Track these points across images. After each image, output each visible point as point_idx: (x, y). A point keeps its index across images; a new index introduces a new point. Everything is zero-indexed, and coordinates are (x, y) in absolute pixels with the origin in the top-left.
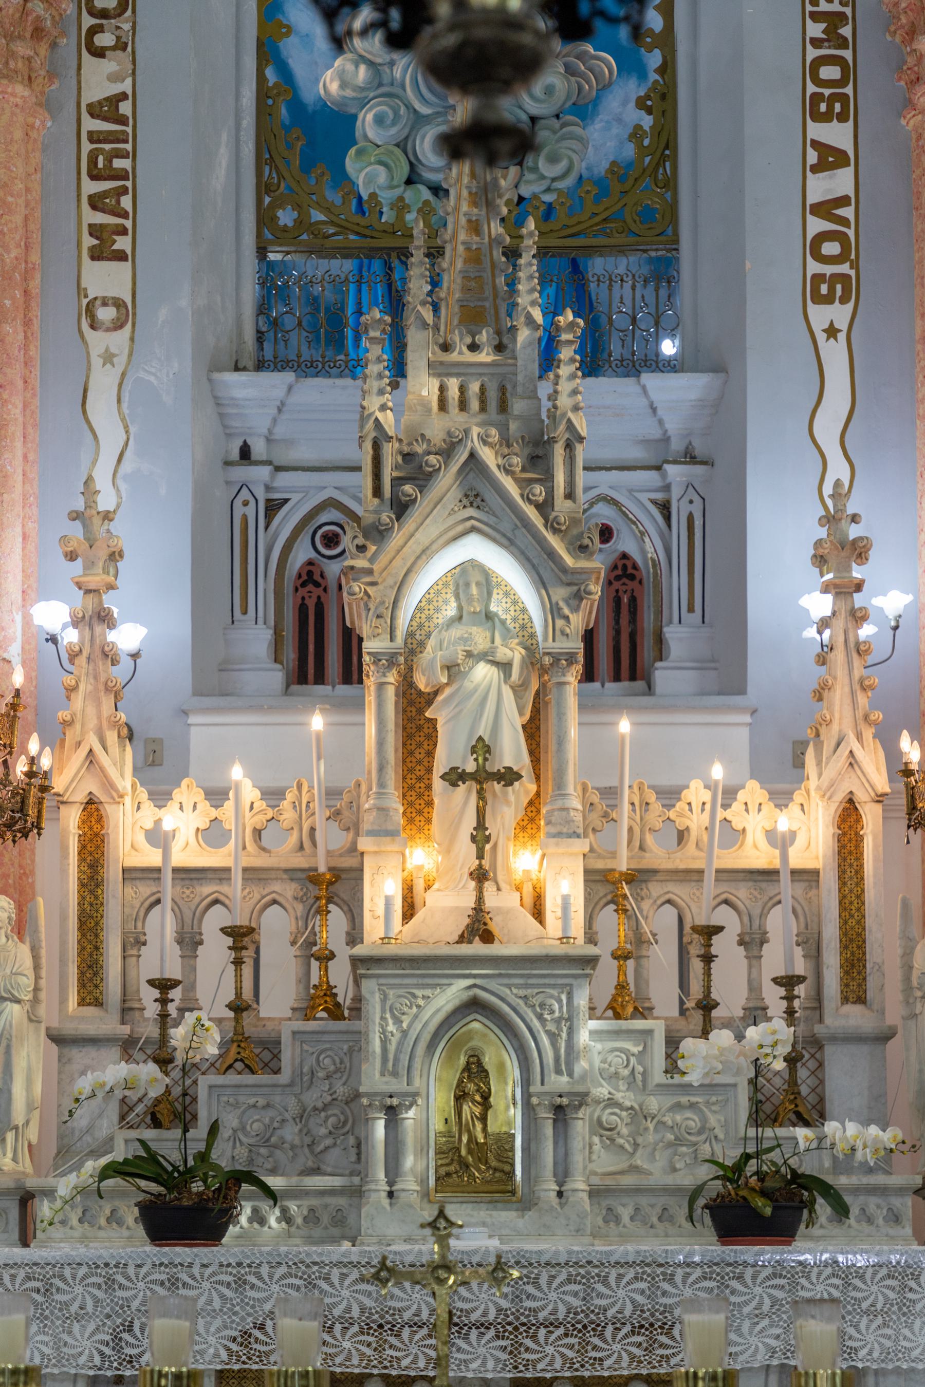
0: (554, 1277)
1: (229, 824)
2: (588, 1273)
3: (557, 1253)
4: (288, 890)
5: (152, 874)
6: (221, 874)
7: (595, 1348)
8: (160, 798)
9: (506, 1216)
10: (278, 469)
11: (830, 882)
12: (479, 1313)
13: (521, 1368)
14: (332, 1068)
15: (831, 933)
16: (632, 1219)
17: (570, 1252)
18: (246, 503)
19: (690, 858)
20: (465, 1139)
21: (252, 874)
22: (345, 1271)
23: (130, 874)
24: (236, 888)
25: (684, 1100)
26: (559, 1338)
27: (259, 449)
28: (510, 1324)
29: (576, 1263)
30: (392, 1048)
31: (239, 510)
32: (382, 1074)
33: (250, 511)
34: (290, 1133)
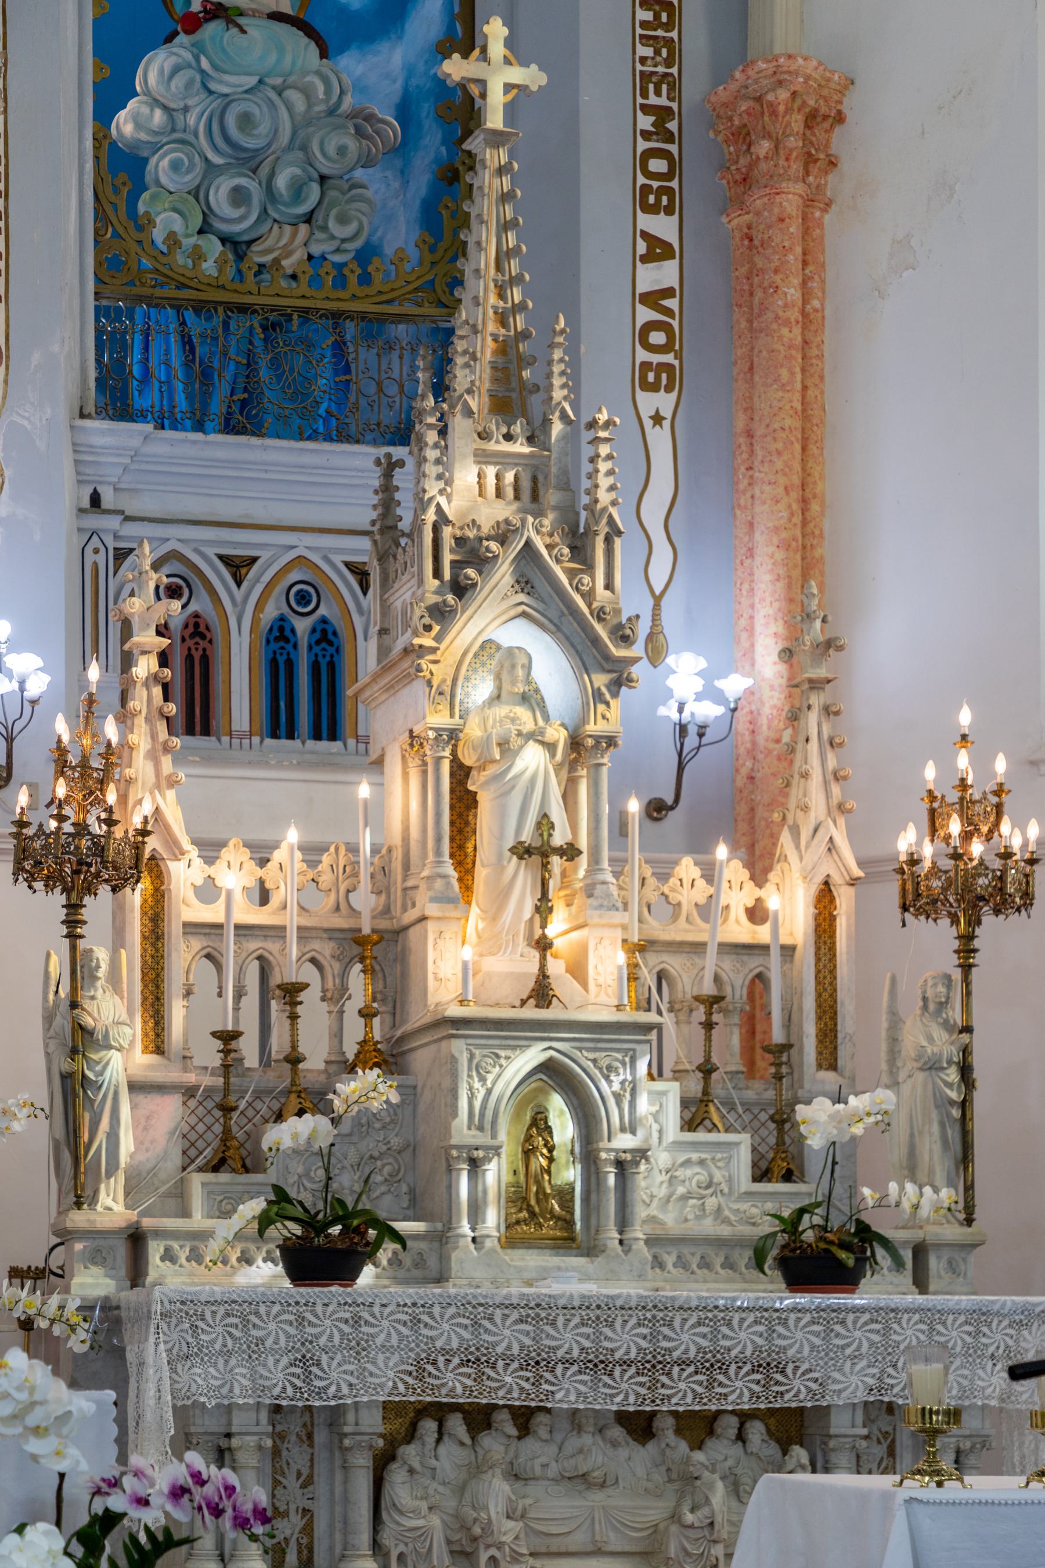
0: (686, 1320)
2: (715, 1316)
3: (689, 1298)
7: (720, 1384)
10: (128, 519)
12: (621, 1352)
13: (658, 1402)
14: (388, 1120)
16: (675, 1266)
17: (699, 1298)
18: (96, 551)
20: (534, 1189)
22: (506, 1312)
25: (695, 1156)
26: (690, 1375)
27: (108, 499)
28: (648, 1362)
29: (644, 1308)
30: (477, 1104)
31: (90, 557)
32: (469, 1128)
33: (101, 558)
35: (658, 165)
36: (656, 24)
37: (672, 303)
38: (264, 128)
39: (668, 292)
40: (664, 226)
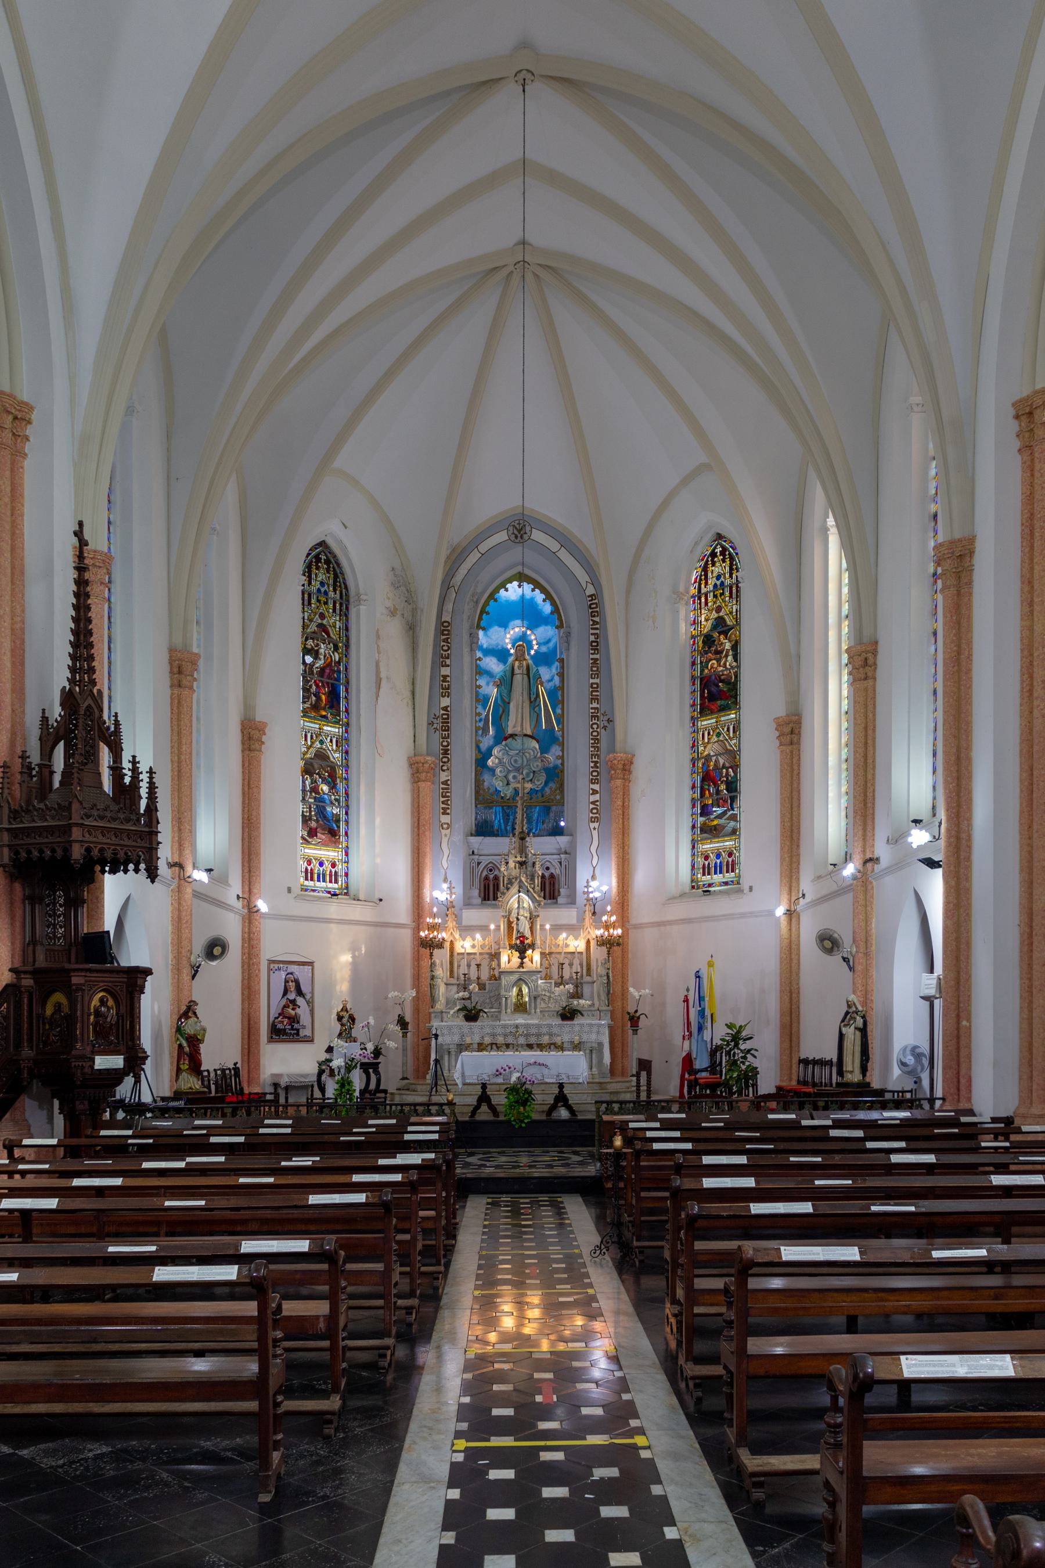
1: (476, 944)
4: (487, 956)
5: (463, 954)
6: (475, 954)
8: (464, 940)
9: (525, 1016)
11: (584, 954)
15: (585, 964)
19: (559, 950)
21: (481, 954)
23: (458, 954)
24: (478, 956)
34: (488, 1001)
35: (595, 774)
36: (595, 743)
37: (598, 803)
38: (520, 762)
39: (597, 801)
40: (596, 787)
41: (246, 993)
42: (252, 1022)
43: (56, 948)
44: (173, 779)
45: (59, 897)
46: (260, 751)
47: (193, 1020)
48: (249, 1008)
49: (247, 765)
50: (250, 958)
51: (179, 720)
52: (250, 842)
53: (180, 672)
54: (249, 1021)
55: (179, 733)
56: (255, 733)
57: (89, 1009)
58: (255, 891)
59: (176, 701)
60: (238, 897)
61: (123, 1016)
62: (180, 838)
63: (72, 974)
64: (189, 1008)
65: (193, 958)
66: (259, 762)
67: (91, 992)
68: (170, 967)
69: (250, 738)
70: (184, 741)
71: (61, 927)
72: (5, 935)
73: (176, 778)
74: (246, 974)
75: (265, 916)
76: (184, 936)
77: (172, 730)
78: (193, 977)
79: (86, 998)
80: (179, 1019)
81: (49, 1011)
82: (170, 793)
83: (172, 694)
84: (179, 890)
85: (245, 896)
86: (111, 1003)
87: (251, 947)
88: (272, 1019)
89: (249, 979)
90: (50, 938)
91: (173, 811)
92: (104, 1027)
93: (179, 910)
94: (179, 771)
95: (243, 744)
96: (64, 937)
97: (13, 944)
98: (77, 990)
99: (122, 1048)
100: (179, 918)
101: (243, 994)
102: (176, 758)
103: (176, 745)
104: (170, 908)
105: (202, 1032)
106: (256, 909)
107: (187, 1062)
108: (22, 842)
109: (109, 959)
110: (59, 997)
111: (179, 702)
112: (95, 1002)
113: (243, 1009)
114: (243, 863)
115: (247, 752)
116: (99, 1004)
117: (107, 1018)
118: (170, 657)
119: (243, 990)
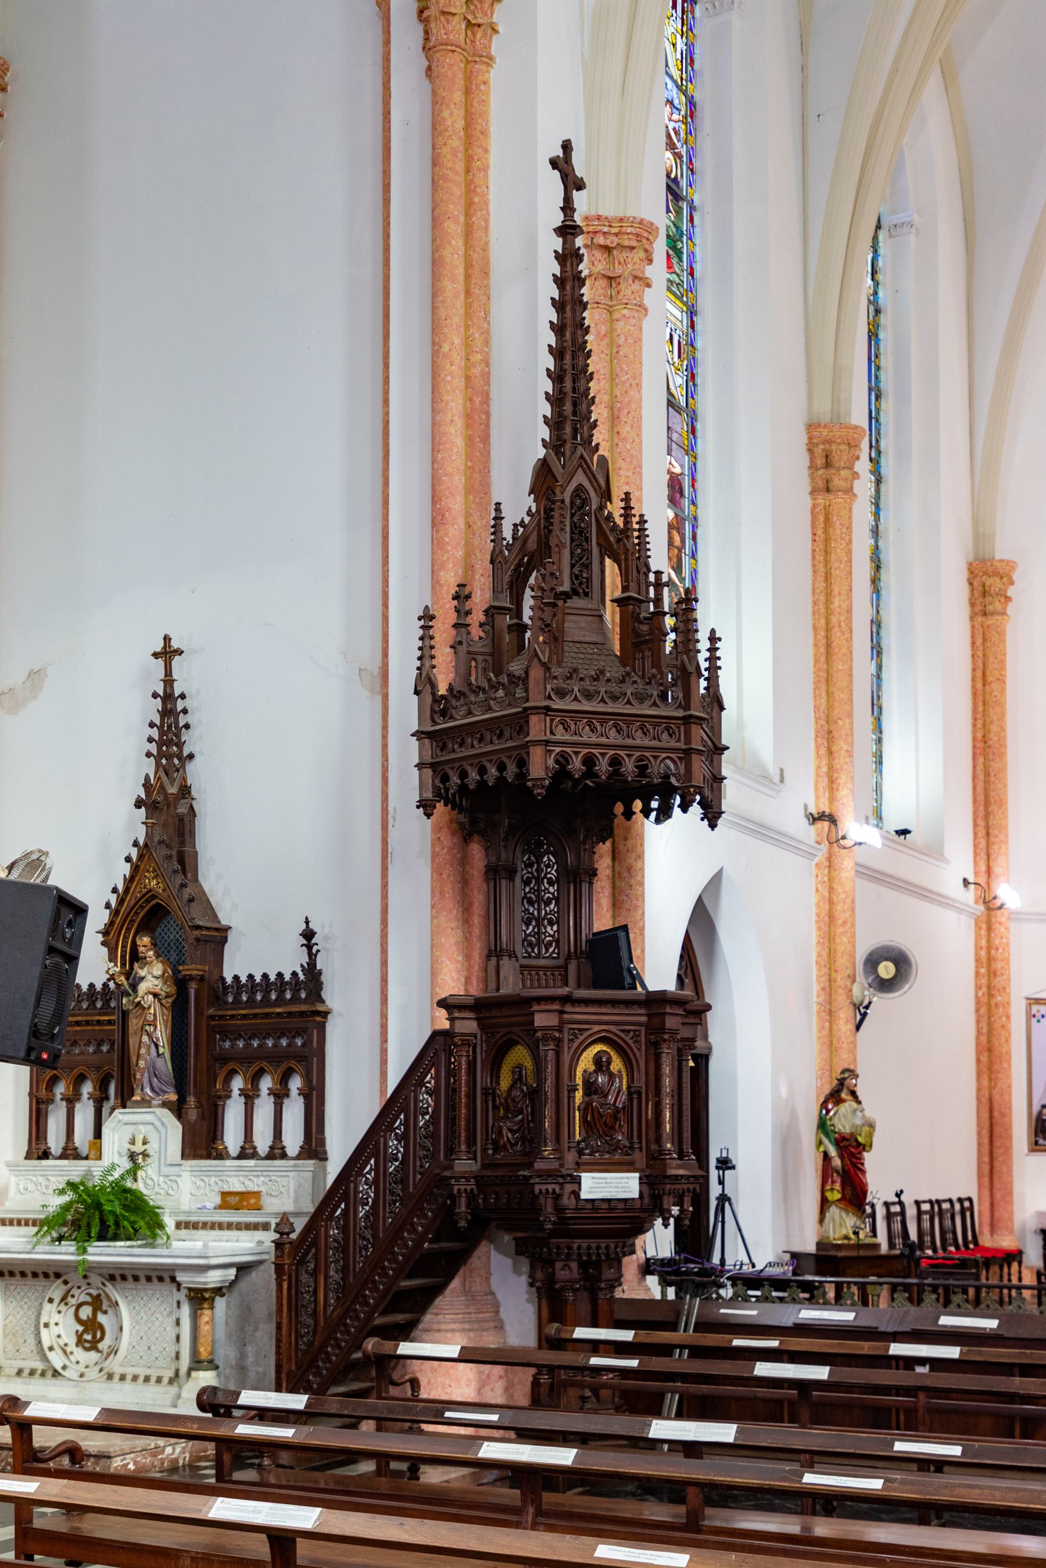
41: (984, 1059)
42: (996, 1114)
43: (542, 962)
44: (817, 661)
45: (548, 866)
46: (1004, 613)
47: (849, 1105)
48: (991, 1088)
49: (979, 642)
50: (991, 996)
51: (826, 552)
52: (987, 782)
53: (828, 465)
54: (991, 1111)
55: (828, 577)
56: (991, 582)
57: (572, 1076)
58: (997, 870)
59: (822, 518)
60: (966, 882)
61: (639, 1093)
62: (831, 768)
63: (535, 1008)
64: (841, 1082)
65: (856, 990)
66: (1002, 634)
67: (576, 1045)
68: (815, 1007)
69: (985, 593)
70: (836, 589)
71: (551, 923)
72: (452, 940)
73: (823, 659)
74: (984, 1024)
75: (1017, 916)
76: (841, 949)
77: (815, 572)
78: (858, 1027)
79: (566, 1057)
80: (824, 1105)
81: (505, 1083)
82: (812, 686)
83: (814, 506)
84: (830, 863)
85: (979, 881)
86: (617, 1065)
87: (992, 974)
88: (1036, 1108)
89: (990, 1033)
90: (530, 944)
91: (817, 719)
92: (601, 1115)
93: (831, 902)
94: (828, 646)
95: (972, 605)
96: (557, 941)
97: (468, 957)
98: (545, 1039)
99: (639, 1157)
100: (831, 916)
101: (978, 1061)
102: (823, 621)
103: (822, 598)
104: (814, 898)
105: (866, 1129)
106: (998, 903)
107: (838, 1186)
108: (452, 756)
109: (628, 980)
110: (520, 1055)
111: (827, 519)
112: (586, 1062)
113: (979, 1090)
114: (975, 820)
115: (980, 619)
116: (592, 1068)
117: (606, 1096)
118: (810, 438)
119: (979, 1053)
